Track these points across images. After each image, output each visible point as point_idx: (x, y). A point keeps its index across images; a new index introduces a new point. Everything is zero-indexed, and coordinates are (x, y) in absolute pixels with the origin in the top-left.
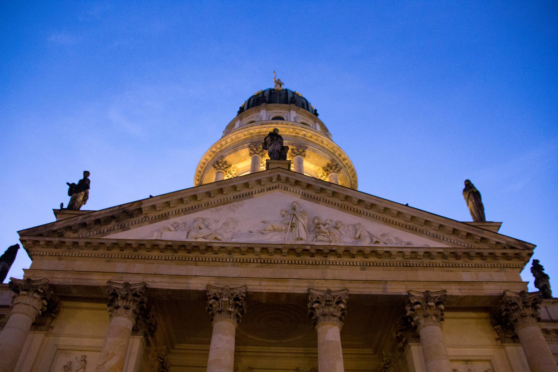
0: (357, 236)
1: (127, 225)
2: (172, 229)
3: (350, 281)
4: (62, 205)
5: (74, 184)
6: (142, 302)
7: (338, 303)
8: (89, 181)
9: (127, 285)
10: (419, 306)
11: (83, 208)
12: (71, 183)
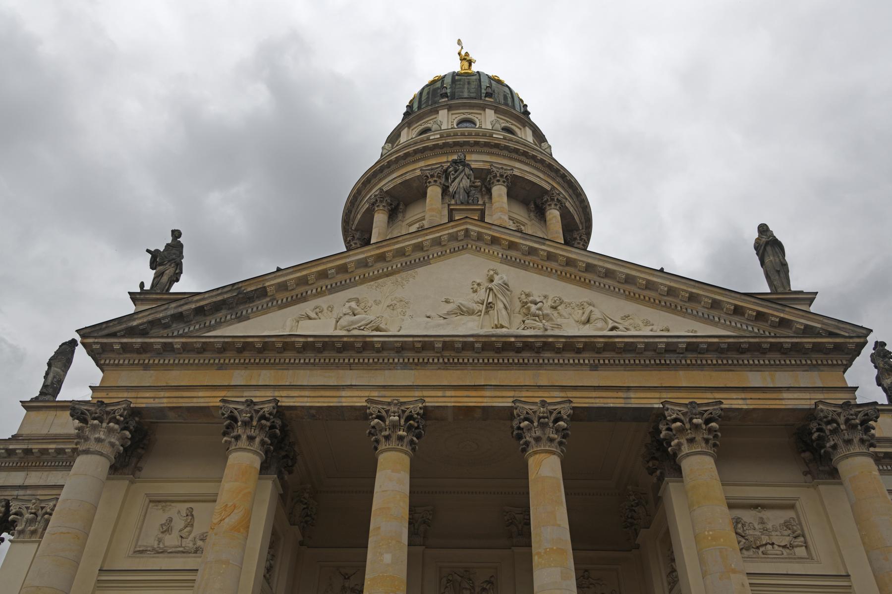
0: (584, 318)
1: (244, 312)
2: (313, 315)
3: (575, 388)
4: (142, 285)
5: (157, 251)
6: (272, 427)
7: (556, 420)
8: (181, 246)
9: (250, 403)
10: (679, 424)
11: (176, 288)
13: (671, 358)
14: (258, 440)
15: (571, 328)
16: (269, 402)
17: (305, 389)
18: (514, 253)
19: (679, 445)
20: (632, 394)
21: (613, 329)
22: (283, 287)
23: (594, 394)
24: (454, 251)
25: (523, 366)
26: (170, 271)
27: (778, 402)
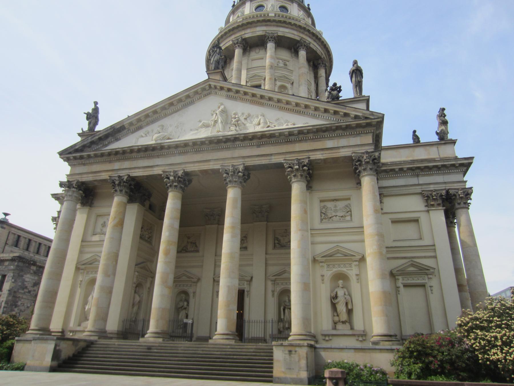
2: (144, 135)
9: (119, 177)
11: (98, 128)
12: (86, 112)
13: (292, 138)
14: (124, 191)
15: (252, 128)
16: (126, 175)
17: (140, 168)
18: (230, 94)
19: (291, 178)
20: (273, 157)
21: (268, 127)
22: (131, 124)
23: (256, 159)
24: (205, 96)
25: (228, 148)
26: (93, 121)
27: (338, 154)
